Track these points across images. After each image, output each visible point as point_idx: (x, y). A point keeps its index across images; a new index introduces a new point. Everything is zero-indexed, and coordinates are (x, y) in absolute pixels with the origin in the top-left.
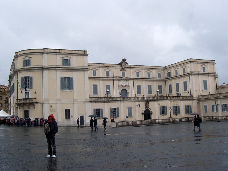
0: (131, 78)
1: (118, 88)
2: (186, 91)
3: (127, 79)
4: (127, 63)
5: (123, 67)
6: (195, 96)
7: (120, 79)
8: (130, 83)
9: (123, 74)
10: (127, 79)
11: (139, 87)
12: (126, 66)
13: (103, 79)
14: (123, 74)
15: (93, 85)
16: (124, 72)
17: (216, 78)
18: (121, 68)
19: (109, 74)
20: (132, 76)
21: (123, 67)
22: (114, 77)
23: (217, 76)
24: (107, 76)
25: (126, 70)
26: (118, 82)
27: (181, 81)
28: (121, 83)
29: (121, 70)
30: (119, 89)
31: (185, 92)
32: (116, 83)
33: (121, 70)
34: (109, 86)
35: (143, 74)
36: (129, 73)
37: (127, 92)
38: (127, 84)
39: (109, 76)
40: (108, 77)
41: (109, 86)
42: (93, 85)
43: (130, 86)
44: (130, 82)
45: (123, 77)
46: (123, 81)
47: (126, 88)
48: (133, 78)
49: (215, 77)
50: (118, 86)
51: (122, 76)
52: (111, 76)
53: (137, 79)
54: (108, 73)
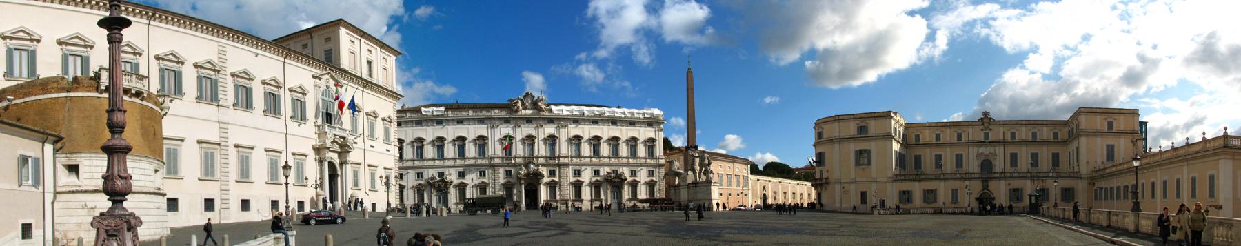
3: (994, 143)
4: (991, 118)
5: (986, 125)
8: (999, 150)
9: (986, 136)
10: (994, 143)
11: (1014, 157)
12: (991, 123)
13: (951, 144)
14: (986, 136)
15: (936, 156)
16: (988, 133)
18: (982, 127)
19: (961, 137)
20: (1002, 138)
21: (986, 125)
24: (958, 140)
25: (991, 129)
26: (976, 149)
28: (981, 150)
29: (982, 130)
30: (978, 159)
32: (974, 151)
33: (982, 130)
35: (1024, 133)
36: (997, 134)
39: (961, 140)
41: (961, 155)
42: (936, 156)
44: (997, 149)
47: (991, 158)
50: (975, 155)
51: (985, 139)
52: (964, 139)
53: (1013, 143)
54: (959, 136)
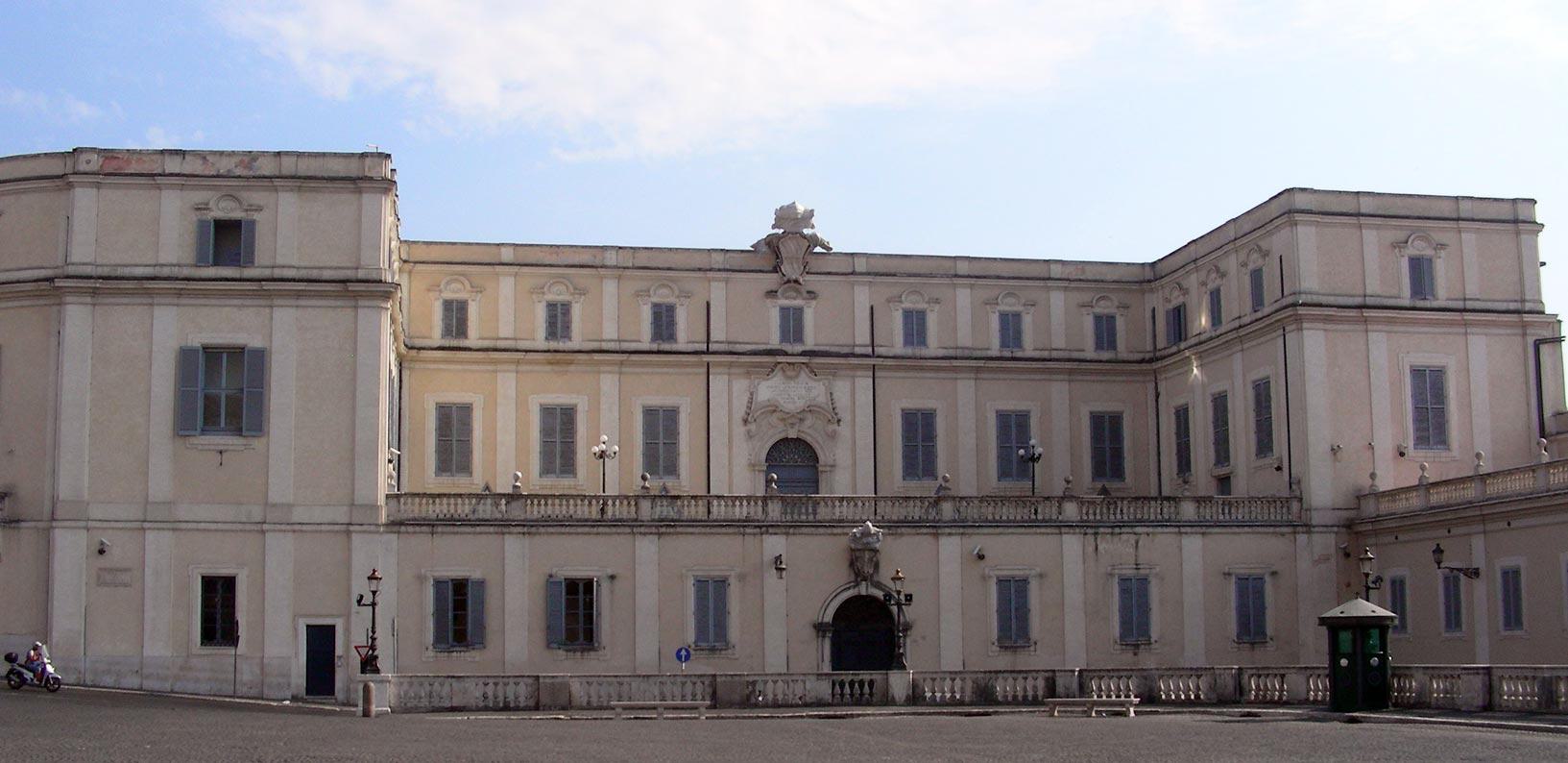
0: (858, 350)
1: (740, 430)
2: (1267, 461)
6: (1323, 489)
7: (767, 361)
17: (1544, 349)
19: (672, 323)
22: (713, 347)
23: (1547, 334)
26: (741, 385)
27: (1238, 378)
30: (750, 436)
31: (1262, 462)
32: (730, 392)
34: (672, 414)
37: (817, 460)
38: (822, 399)
40: (666, 347)
41: (672, 414)
43: (846, 416)
44: (842, 388)
45: (788, 348)
46: (790, 378)
47: (811, 431)
48: (869, 350)
49: (1530, 340)
52: (686, 332)
53: (911, 364)
